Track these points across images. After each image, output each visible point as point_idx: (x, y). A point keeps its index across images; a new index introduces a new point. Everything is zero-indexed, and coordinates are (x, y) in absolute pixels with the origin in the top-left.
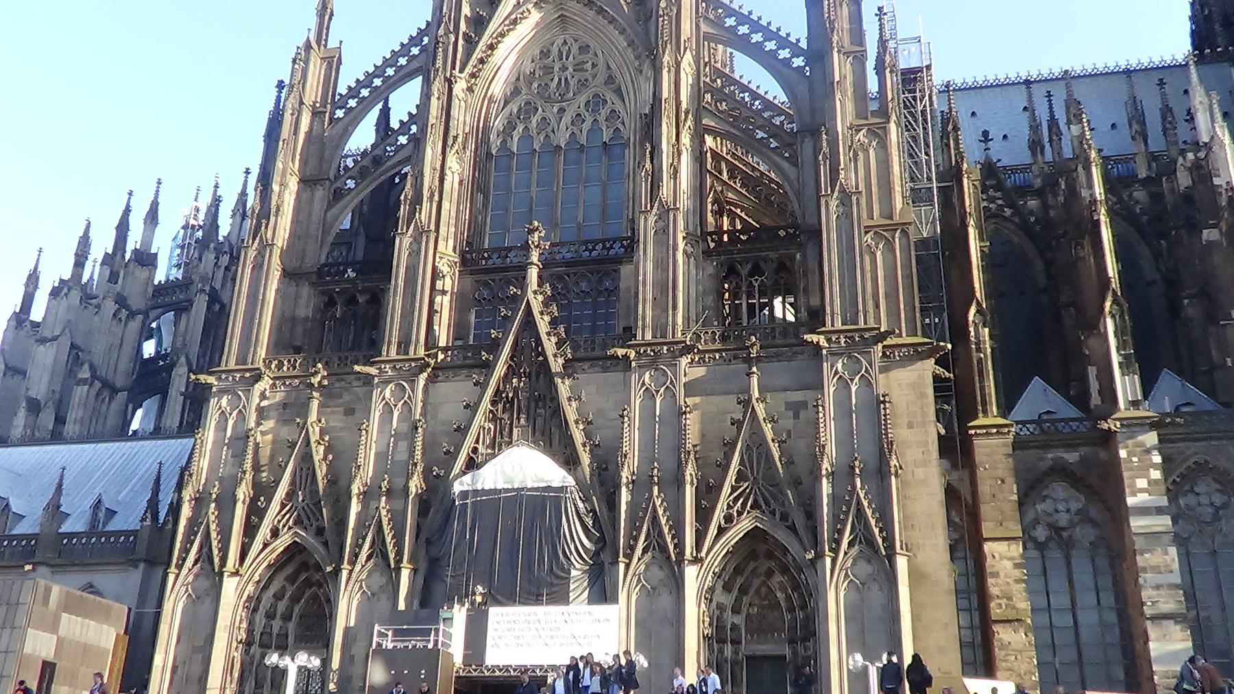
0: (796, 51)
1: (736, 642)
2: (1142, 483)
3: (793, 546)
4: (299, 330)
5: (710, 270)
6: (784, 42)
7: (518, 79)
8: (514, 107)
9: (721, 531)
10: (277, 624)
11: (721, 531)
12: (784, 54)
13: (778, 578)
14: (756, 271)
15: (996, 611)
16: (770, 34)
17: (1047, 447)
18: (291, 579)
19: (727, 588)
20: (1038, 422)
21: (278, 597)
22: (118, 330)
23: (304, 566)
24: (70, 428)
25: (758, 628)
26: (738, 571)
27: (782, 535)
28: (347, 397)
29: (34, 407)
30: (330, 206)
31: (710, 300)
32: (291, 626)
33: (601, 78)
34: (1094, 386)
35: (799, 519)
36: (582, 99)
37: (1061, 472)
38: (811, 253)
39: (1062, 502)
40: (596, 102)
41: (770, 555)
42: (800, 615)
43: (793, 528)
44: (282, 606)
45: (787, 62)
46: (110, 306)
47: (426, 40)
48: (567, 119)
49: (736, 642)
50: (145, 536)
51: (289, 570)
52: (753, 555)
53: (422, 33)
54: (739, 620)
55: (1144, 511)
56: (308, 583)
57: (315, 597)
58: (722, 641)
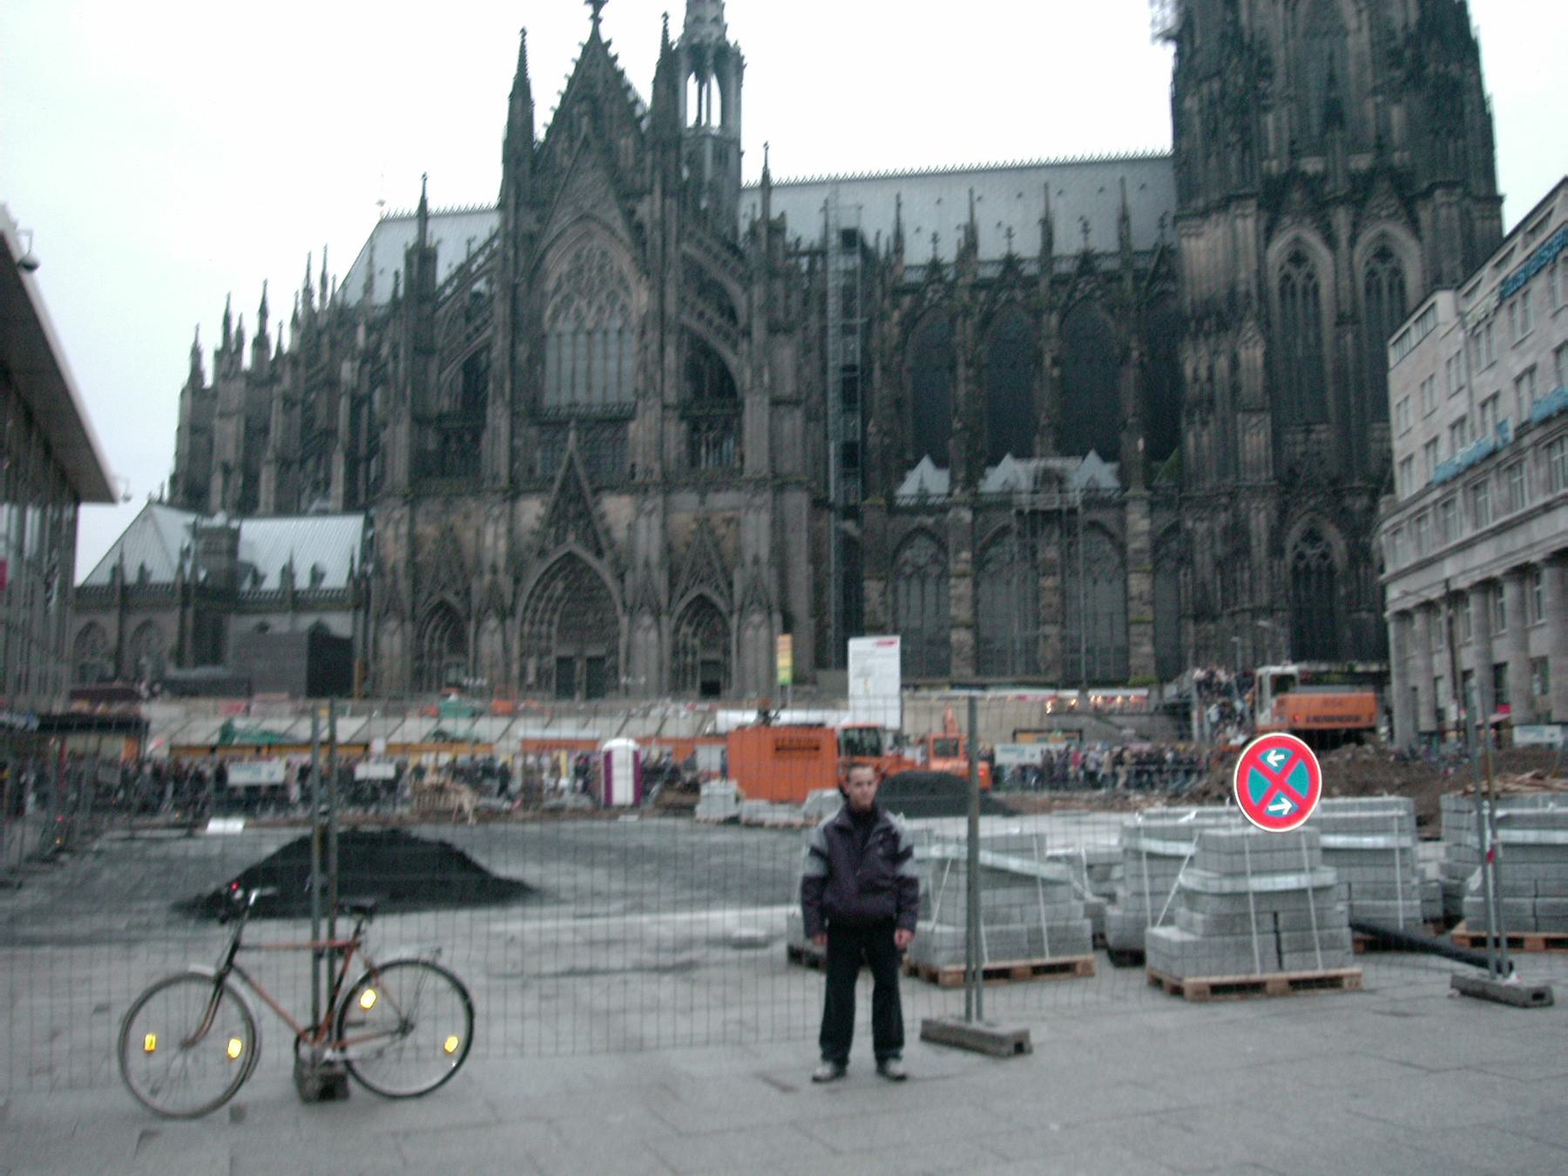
5: (684, 426)
7: (559, 278)
8: (558, 299)
13: (716, 619)
19: (690, 623)
21: (436, 628)
25: (706, 645)
26: (695, 614)
27: (716, 598)
29: (227, 470)
30: (440, 373)
31: (683, 447)
32: (445, 644)
36: (604, 295)
37: (922, 530)
40: (613, 296)
43: (721, 593)
44: (438, 633)
47: (496, 244)
49: (694, 654)
54: (697, 642)
56: (450, 621)
58: (686, 654)
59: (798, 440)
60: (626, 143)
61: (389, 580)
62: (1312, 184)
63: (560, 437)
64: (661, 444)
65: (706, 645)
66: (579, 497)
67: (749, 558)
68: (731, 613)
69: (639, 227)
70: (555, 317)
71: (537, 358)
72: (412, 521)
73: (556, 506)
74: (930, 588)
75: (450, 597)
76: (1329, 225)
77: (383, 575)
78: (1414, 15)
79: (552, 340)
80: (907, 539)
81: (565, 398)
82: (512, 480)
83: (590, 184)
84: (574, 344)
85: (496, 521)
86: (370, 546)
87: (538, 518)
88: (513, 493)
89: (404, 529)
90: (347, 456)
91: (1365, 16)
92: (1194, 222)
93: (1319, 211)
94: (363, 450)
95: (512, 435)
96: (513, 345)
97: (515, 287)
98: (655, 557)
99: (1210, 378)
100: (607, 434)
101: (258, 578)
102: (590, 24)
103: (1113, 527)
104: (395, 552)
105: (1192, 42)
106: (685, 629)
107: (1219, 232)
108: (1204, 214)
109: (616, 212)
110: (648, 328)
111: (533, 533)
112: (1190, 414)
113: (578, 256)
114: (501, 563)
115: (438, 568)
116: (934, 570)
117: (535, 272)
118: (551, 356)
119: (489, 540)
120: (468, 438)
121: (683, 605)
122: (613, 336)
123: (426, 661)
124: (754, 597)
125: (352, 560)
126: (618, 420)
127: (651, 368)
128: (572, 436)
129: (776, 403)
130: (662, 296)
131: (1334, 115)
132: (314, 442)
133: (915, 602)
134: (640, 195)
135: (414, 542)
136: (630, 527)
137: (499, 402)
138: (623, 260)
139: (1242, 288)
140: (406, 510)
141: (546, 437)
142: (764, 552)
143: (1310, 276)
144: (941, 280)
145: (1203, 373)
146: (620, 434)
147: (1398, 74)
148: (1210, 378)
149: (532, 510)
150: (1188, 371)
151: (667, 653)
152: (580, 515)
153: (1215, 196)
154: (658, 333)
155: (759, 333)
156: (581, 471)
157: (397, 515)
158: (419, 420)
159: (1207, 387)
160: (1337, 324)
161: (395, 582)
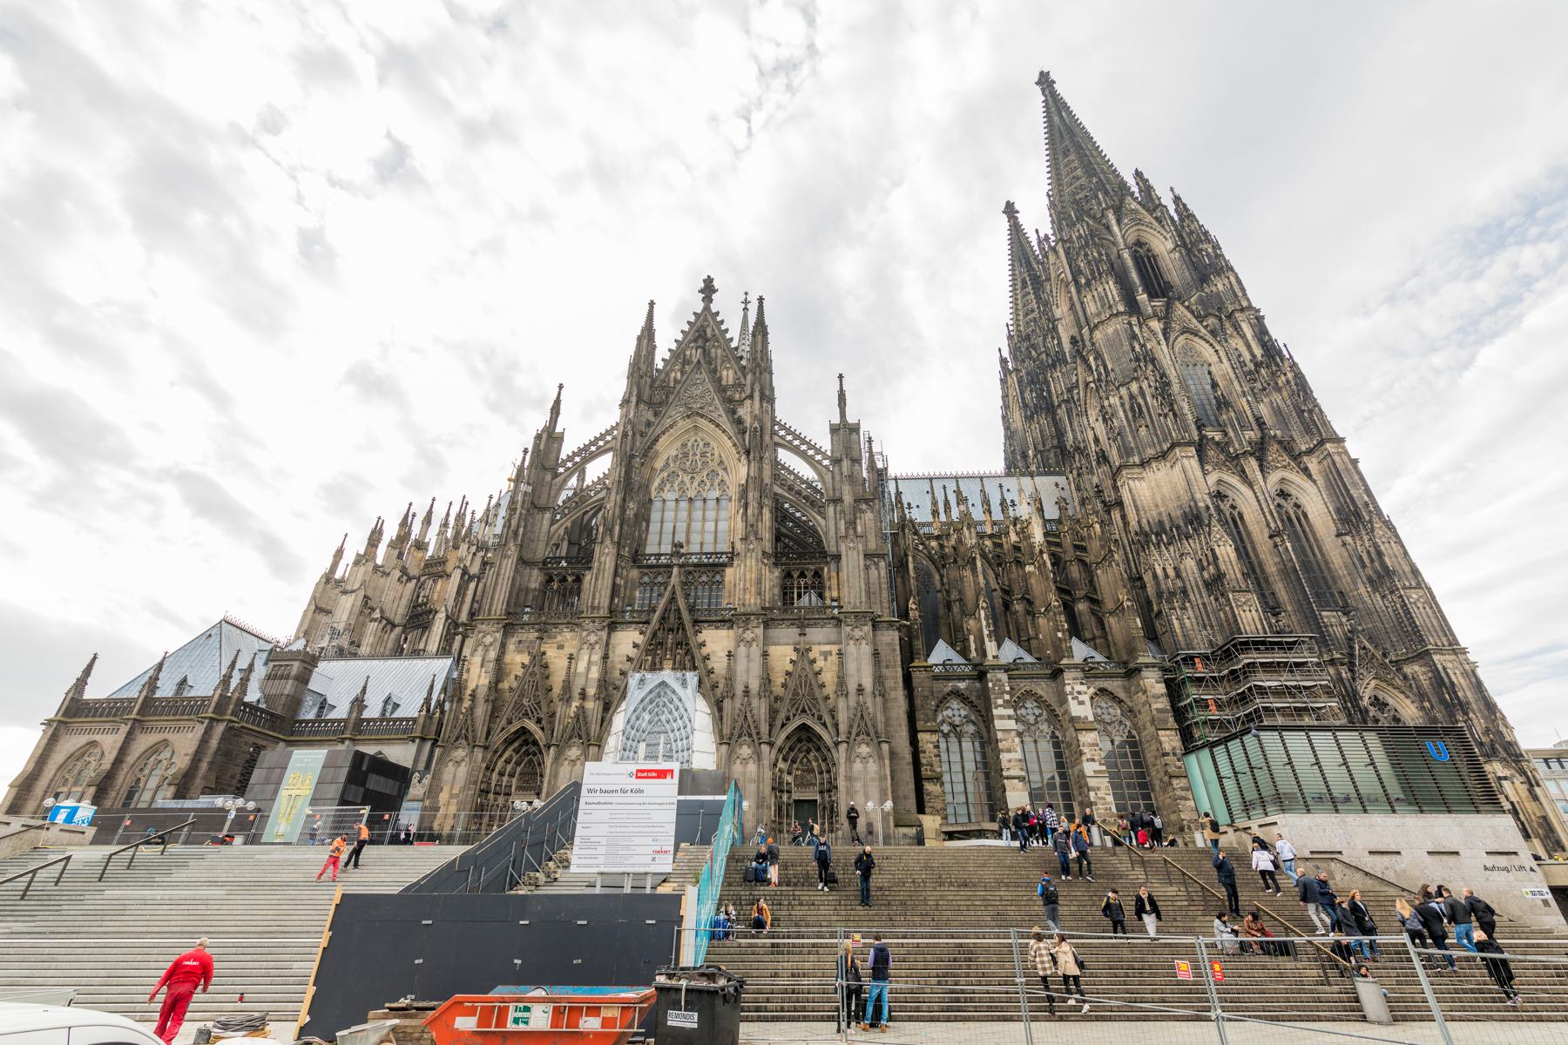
0: (825, 457)
1: (789, 792)
2: (1000, 702)
3: (825, 736)
4: (530, 596)
6: (818, 451)
8: (665, 474)
9: (783, 725)
10: (505, 779)
11: (783, 725)
12: (818, 457)
14: (802, 575)
15: (925, 772)
16: (813, 447)
17: (948, 678)
18: (516, 751)
19: (785, 760)
20: (944, 664)
21: (507, 762)
22: (400, 588)
23: (526, 742)
24: (364, 650)
26: (791, 749)
27: (818, 729)
28: (559, 638)
31: (776, 591)
32: (514, 781)
33: (717, 461)
34: (973, 646)
35: (827, 718)
37: (956, 693)
38: (833, 566)
39: (956, 711)
41: (809, 740)
42: (825, 775)
43: (824, 724)
44: (509, 768)
45: (819, 462)
46: (397, 574)
48: (696, 484)
49: (789, 792)
50: (421, 721)
51: (516, 745)
52: (800, 740)
53: (613, 428)
55: (1002, 717)
56: (527, 753)
57: (531, 761)
59: (884, 586)
60: (728, 376)
61: (467, 704)
62: (1222, 447)
63: (660, 579)
64: (759, 582)
65: (802, 784)
66: (681, 626)
67: (852, 688)
68: (837, 744)
69: (740, 421)
70: (661, 489)
71: (643, 517)
72: (503, 646)
73: (654, 635)
74: (967, 745)
75: (531, 725)
76: (1243, 471)
77: (461, 700)
78: (1258, 352)
79: (657, 505)
80: (942, 702)
81: (667, 548)
82: (611, 612)
83: (702, 386)
84: (676, 510)
85: (592, 646)
86: (455, 688)
87: (635, 646)
88: (613, 624)
89: (492, 655)
90: (448, 617)
91: (1222, 354)
92: (1137, 470)
93: (1234, 462)
94: (464, 617)
95: (616, 574)
96: (624, 500)
97: (632, 457)
98: (755, 685)
99: (1178, 575)
100: (704, 578)
101: (323, 705)
102: (702, 305)
103: (1122, 695)
104: (478, 677)
105: (1105, 367)
106: (781, 765)
107: (1159, 475)
108: (1144, 464)
109: (722, 412)
110: (751, 486)
111: (629, 659)
112: (1169, 602)
113: (684, 445)
114: (591, 691)
115: (522, 696)
116: (971, 729)
117: (648, 451)
118: (655, 516)
119: (582, 666)
120: (570, 579)
121: (783, 736)
122: (711, 504)
123: (491, 796)
124: (865, 729)
125: (432, 687)
126: (714, 567)
127: (751, 519)
128: (675, 570)
129: (866, 556)
130: (761, 469)
131: (1223, 404)
132: (419, 618)
133: (955, 757)
134: (741, 402)
135: (500, 671)
136: (730, 655)
137: (608, 541)
138: (724, 445)
139: (1201, 504)
140: (499, 636)
141: (646, 579)
142: (868, 683)
143: (1233, 507)
144: (916, 533)
145: (1171, 572)
146: (718, 578)
147: (1258, 385)
148: (1178, 575)
149: (628, 641)
150: (1159, 571)
151: (767, 790)
152: (679, 644)
153: (1150, 452)
154: (757, 494)
155: (848, 498)
156: (681, 603)
157: (489, 639)
158: (523, 561)
159: (1180, 584)
160: (1271, 537)
161: (472, 709)
